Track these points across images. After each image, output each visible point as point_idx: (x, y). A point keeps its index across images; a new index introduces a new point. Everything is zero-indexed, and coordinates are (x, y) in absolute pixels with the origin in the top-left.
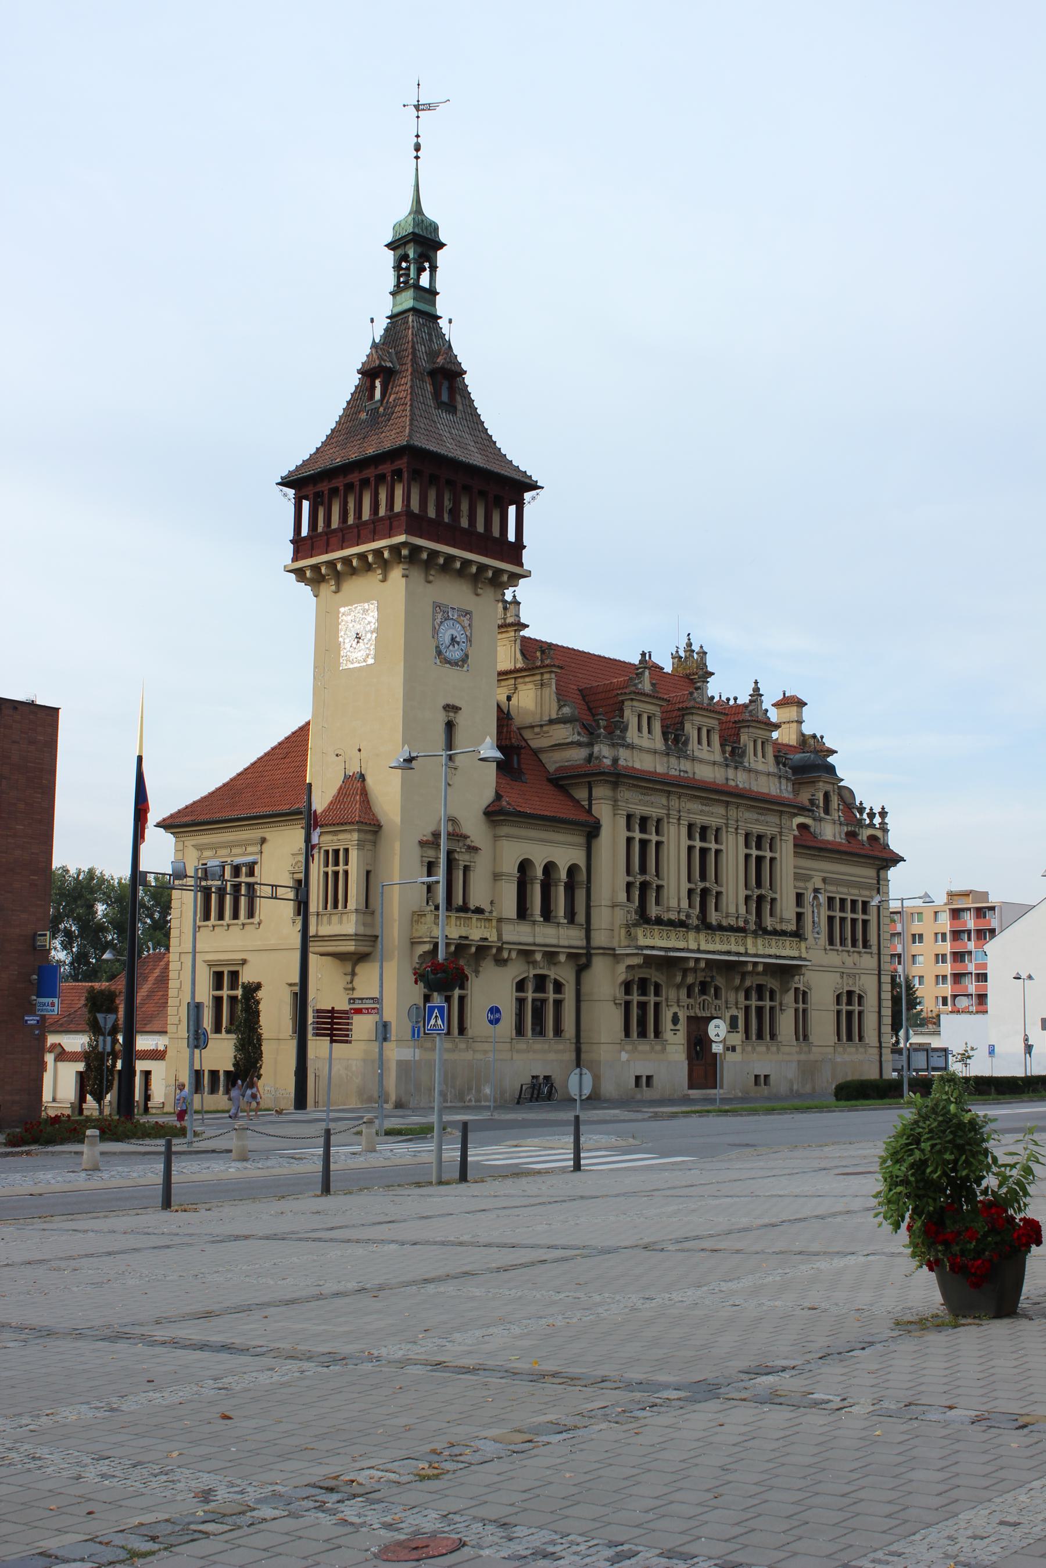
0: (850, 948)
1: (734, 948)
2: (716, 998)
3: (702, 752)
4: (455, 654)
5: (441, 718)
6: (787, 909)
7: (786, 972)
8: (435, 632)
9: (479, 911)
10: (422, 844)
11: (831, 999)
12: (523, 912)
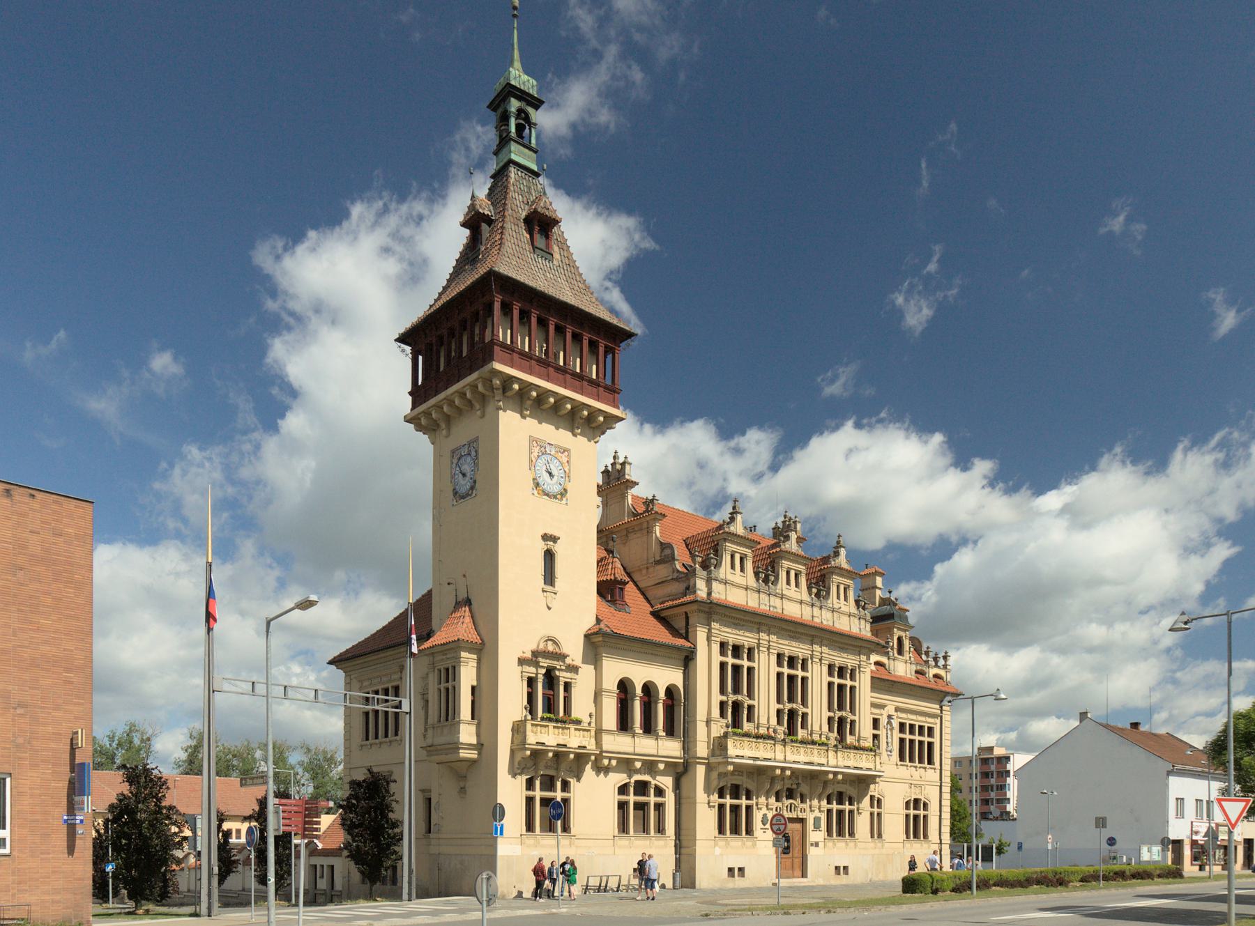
0: (917, 764)
1: (816, 760)
2: (802, 802)
3: (791, 592)
4: (552, 486)
5: (541, 546)
6: (866, 730)
7: (862, 782)
8: (532, 465)
9: (578, 722)
10: (522, 662)
11: (902, 805)
12: (624, 724)
